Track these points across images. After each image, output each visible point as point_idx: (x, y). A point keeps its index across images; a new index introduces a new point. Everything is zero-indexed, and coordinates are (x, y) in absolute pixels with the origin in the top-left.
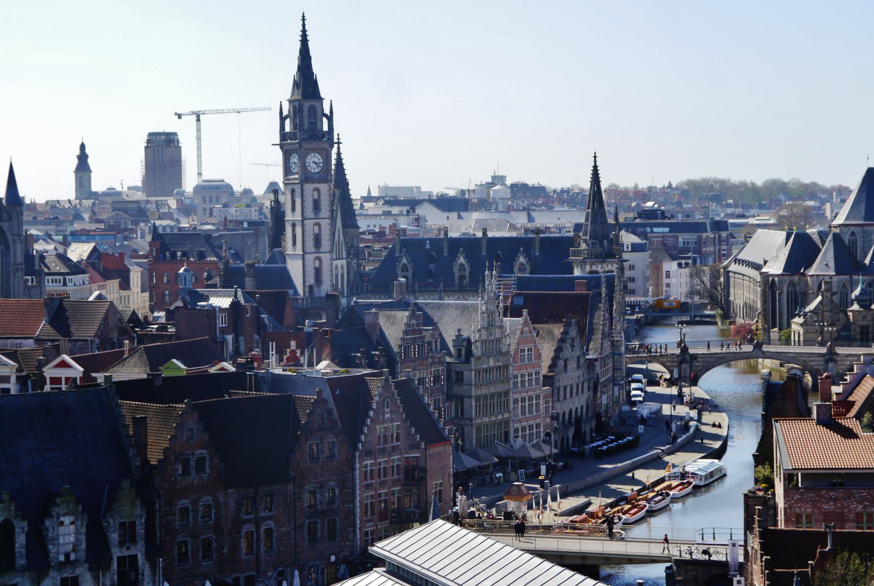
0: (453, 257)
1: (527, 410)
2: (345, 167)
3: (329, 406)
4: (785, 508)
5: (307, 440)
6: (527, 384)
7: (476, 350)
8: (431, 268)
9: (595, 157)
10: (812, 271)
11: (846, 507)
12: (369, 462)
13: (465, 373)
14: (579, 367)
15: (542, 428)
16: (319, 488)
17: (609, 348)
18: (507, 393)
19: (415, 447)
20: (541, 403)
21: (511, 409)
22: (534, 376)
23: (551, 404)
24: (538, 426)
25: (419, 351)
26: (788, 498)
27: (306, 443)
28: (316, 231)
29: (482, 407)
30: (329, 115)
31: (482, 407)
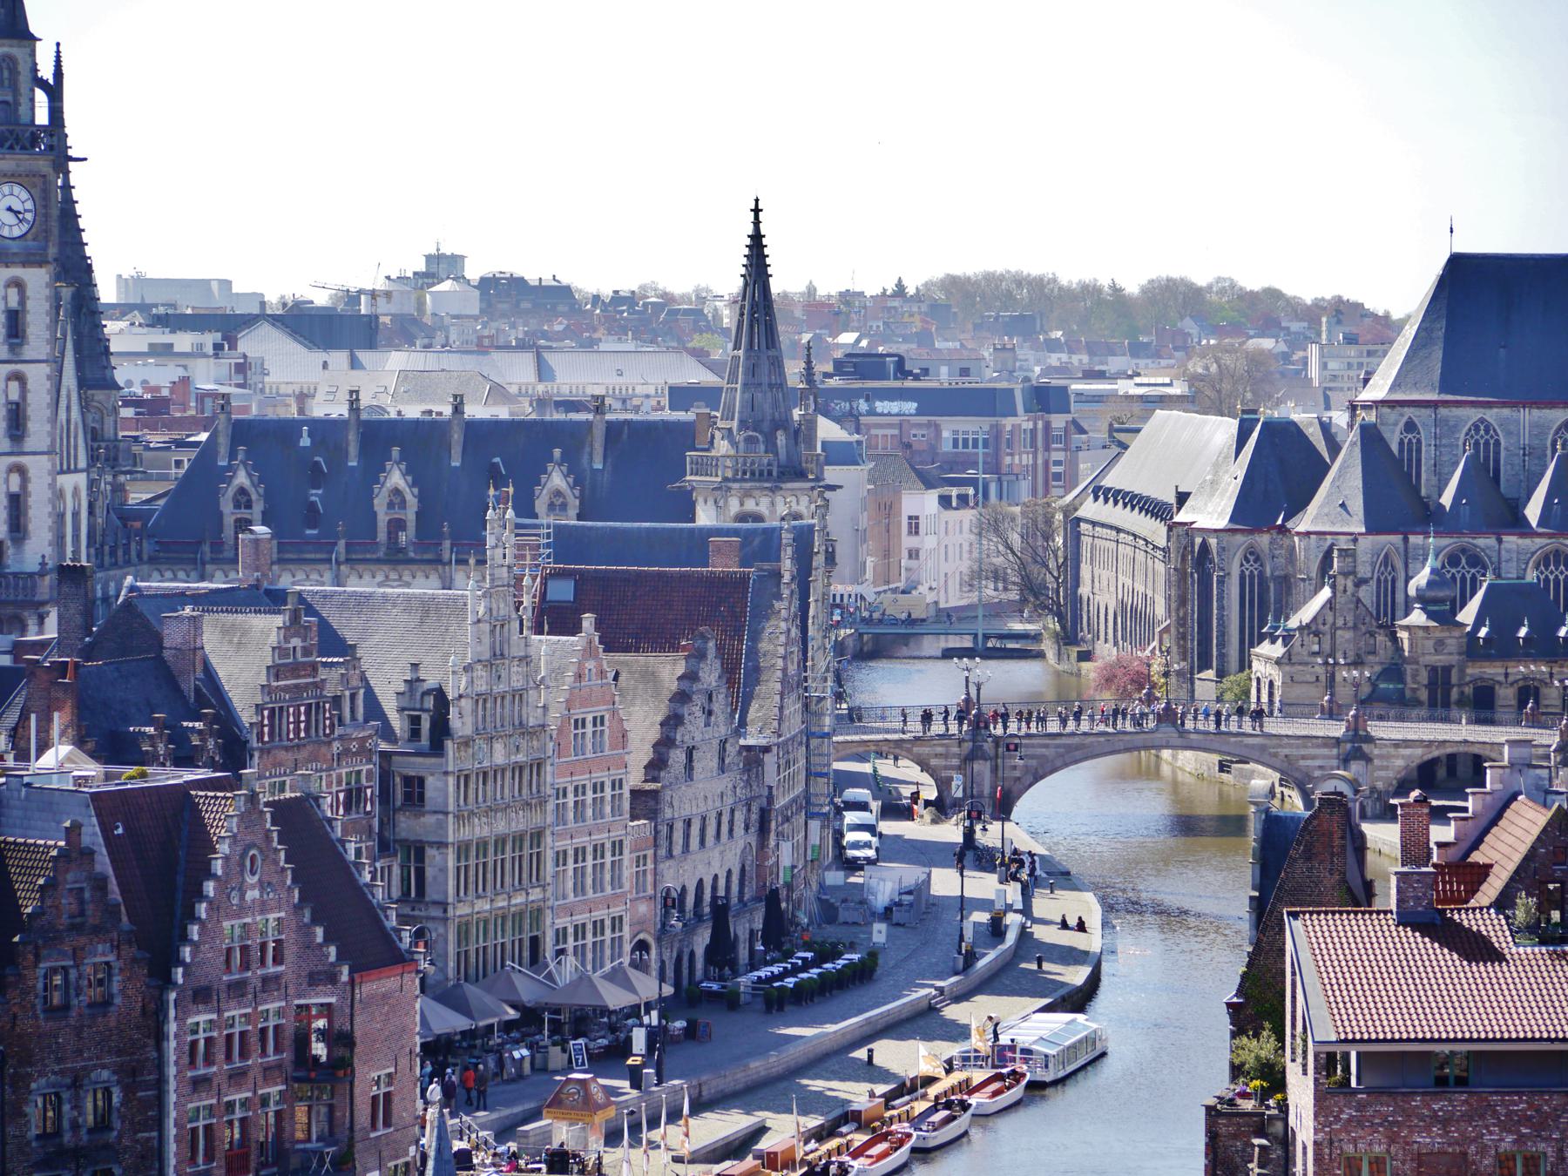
0: (373, 470)
1: (589, 881)
2: (82, 223)
3: (98, 868)
4: (1315, 1143)
5: (38, 958)
6: (589, 812)
7: (461, 721)
8: (313, 498)
9: (757, 211)
10: (1304, 522)
11: (1474, 1140)
12: (202, 1018)
13: (431, 782)
14: (722, 768)
15: (626, 928)
16: (69, 1088)
17: (798, 718)
18: (537, 836)
19: (322, 977)
20: (626, 863)
21: (549, 879)
22: (608, 791)
23: (650, 866)
24: (617, 923)
25: (308, 721)
26: (1326, 1116)
27: (36, 966)
28: (14, 395)
29: (472, 872)
30: (51, 81)
31: (472, 872)
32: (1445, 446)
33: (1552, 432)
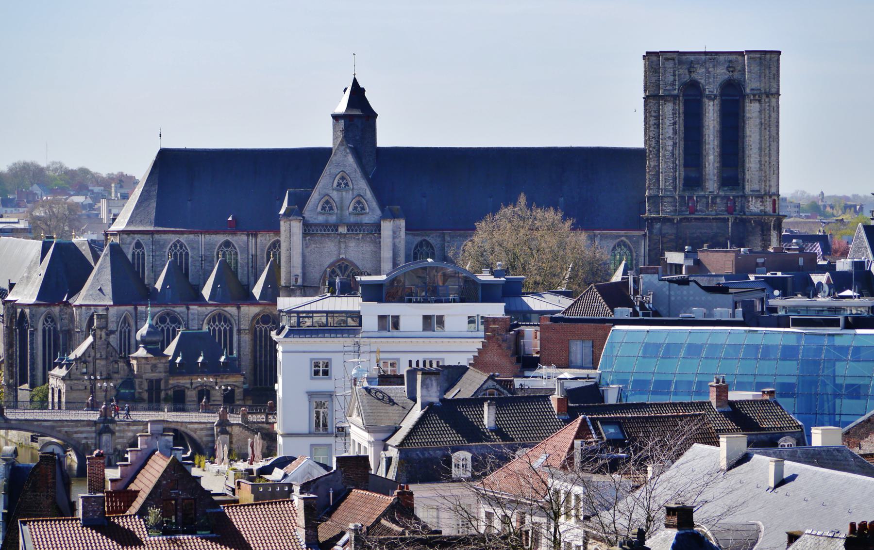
10: (79, 299)
32: (158, 256)
33: (217, 247)
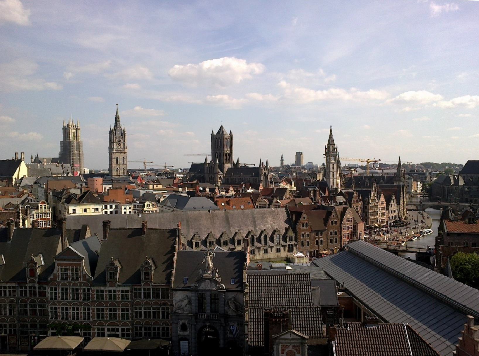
13: (367, 207)
24: (385, 219)
